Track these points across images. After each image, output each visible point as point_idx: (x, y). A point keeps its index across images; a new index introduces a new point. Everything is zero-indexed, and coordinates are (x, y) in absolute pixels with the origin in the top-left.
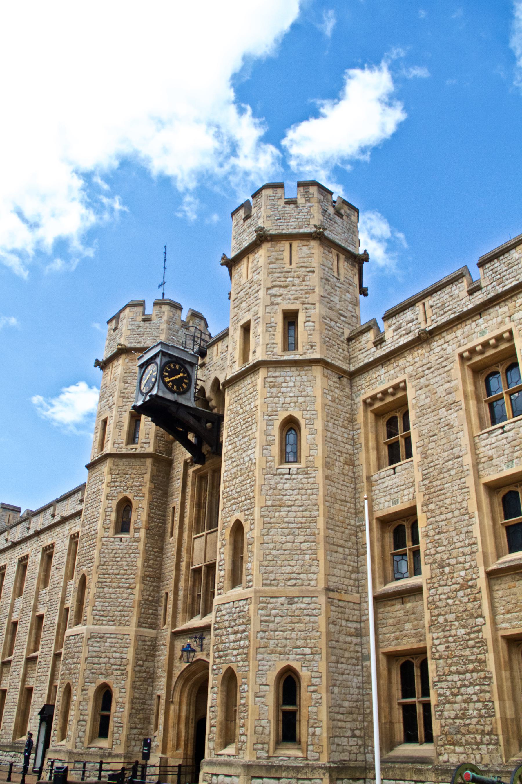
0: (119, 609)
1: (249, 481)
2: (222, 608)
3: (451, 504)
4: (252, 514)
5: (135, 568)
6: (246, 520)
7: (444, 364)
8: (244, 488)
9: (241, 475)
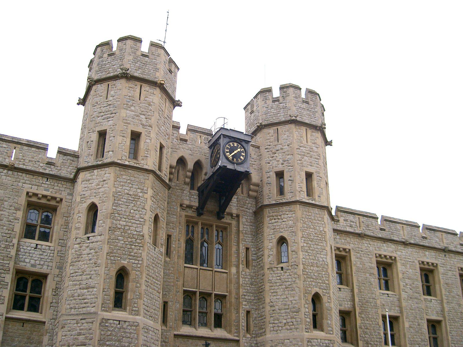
0: (154, 307)
1: (323, 273)
2: (312, 341)
3: (372, 318)
4: (329, 293)
5: (160, 277)
6: (324, 295)
7: (369, 253)
8: (320, 275)
9: (316, 267)
